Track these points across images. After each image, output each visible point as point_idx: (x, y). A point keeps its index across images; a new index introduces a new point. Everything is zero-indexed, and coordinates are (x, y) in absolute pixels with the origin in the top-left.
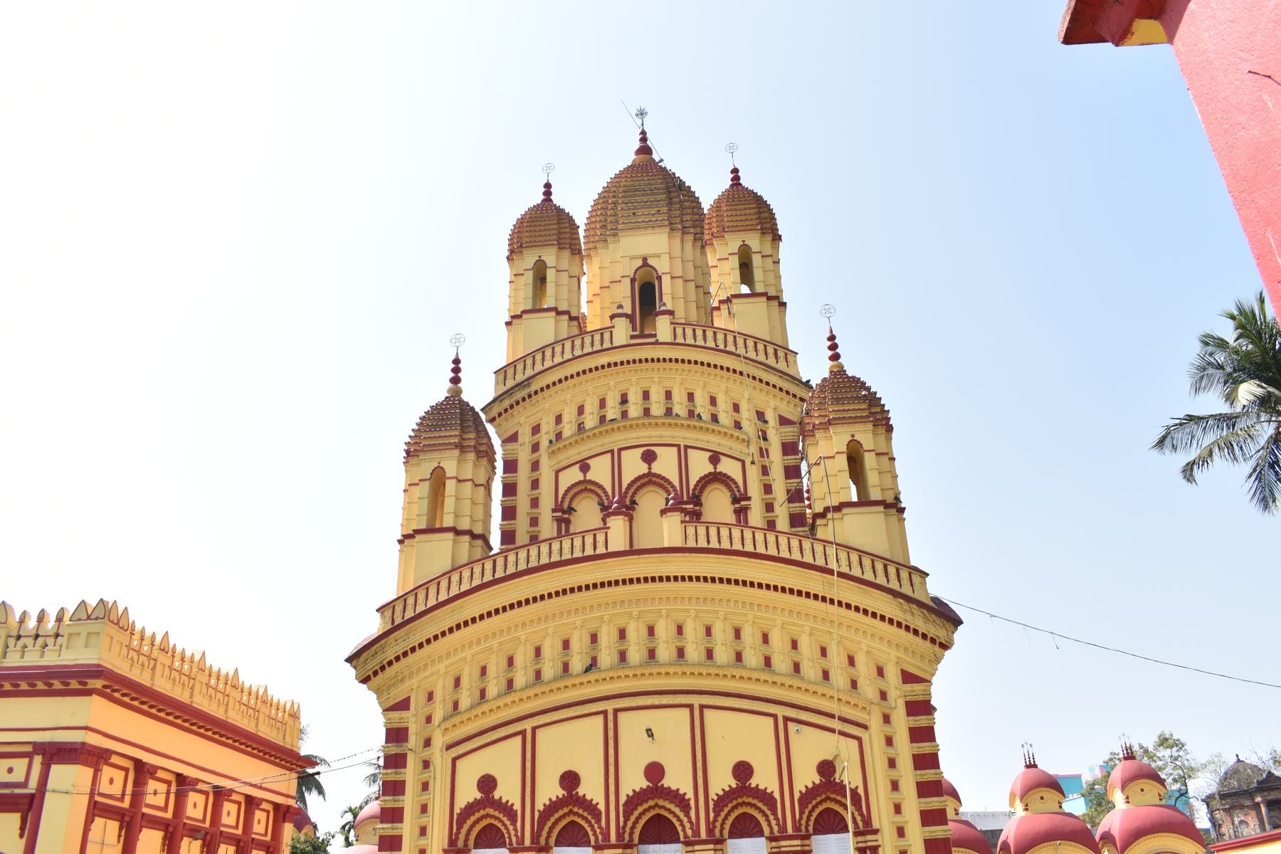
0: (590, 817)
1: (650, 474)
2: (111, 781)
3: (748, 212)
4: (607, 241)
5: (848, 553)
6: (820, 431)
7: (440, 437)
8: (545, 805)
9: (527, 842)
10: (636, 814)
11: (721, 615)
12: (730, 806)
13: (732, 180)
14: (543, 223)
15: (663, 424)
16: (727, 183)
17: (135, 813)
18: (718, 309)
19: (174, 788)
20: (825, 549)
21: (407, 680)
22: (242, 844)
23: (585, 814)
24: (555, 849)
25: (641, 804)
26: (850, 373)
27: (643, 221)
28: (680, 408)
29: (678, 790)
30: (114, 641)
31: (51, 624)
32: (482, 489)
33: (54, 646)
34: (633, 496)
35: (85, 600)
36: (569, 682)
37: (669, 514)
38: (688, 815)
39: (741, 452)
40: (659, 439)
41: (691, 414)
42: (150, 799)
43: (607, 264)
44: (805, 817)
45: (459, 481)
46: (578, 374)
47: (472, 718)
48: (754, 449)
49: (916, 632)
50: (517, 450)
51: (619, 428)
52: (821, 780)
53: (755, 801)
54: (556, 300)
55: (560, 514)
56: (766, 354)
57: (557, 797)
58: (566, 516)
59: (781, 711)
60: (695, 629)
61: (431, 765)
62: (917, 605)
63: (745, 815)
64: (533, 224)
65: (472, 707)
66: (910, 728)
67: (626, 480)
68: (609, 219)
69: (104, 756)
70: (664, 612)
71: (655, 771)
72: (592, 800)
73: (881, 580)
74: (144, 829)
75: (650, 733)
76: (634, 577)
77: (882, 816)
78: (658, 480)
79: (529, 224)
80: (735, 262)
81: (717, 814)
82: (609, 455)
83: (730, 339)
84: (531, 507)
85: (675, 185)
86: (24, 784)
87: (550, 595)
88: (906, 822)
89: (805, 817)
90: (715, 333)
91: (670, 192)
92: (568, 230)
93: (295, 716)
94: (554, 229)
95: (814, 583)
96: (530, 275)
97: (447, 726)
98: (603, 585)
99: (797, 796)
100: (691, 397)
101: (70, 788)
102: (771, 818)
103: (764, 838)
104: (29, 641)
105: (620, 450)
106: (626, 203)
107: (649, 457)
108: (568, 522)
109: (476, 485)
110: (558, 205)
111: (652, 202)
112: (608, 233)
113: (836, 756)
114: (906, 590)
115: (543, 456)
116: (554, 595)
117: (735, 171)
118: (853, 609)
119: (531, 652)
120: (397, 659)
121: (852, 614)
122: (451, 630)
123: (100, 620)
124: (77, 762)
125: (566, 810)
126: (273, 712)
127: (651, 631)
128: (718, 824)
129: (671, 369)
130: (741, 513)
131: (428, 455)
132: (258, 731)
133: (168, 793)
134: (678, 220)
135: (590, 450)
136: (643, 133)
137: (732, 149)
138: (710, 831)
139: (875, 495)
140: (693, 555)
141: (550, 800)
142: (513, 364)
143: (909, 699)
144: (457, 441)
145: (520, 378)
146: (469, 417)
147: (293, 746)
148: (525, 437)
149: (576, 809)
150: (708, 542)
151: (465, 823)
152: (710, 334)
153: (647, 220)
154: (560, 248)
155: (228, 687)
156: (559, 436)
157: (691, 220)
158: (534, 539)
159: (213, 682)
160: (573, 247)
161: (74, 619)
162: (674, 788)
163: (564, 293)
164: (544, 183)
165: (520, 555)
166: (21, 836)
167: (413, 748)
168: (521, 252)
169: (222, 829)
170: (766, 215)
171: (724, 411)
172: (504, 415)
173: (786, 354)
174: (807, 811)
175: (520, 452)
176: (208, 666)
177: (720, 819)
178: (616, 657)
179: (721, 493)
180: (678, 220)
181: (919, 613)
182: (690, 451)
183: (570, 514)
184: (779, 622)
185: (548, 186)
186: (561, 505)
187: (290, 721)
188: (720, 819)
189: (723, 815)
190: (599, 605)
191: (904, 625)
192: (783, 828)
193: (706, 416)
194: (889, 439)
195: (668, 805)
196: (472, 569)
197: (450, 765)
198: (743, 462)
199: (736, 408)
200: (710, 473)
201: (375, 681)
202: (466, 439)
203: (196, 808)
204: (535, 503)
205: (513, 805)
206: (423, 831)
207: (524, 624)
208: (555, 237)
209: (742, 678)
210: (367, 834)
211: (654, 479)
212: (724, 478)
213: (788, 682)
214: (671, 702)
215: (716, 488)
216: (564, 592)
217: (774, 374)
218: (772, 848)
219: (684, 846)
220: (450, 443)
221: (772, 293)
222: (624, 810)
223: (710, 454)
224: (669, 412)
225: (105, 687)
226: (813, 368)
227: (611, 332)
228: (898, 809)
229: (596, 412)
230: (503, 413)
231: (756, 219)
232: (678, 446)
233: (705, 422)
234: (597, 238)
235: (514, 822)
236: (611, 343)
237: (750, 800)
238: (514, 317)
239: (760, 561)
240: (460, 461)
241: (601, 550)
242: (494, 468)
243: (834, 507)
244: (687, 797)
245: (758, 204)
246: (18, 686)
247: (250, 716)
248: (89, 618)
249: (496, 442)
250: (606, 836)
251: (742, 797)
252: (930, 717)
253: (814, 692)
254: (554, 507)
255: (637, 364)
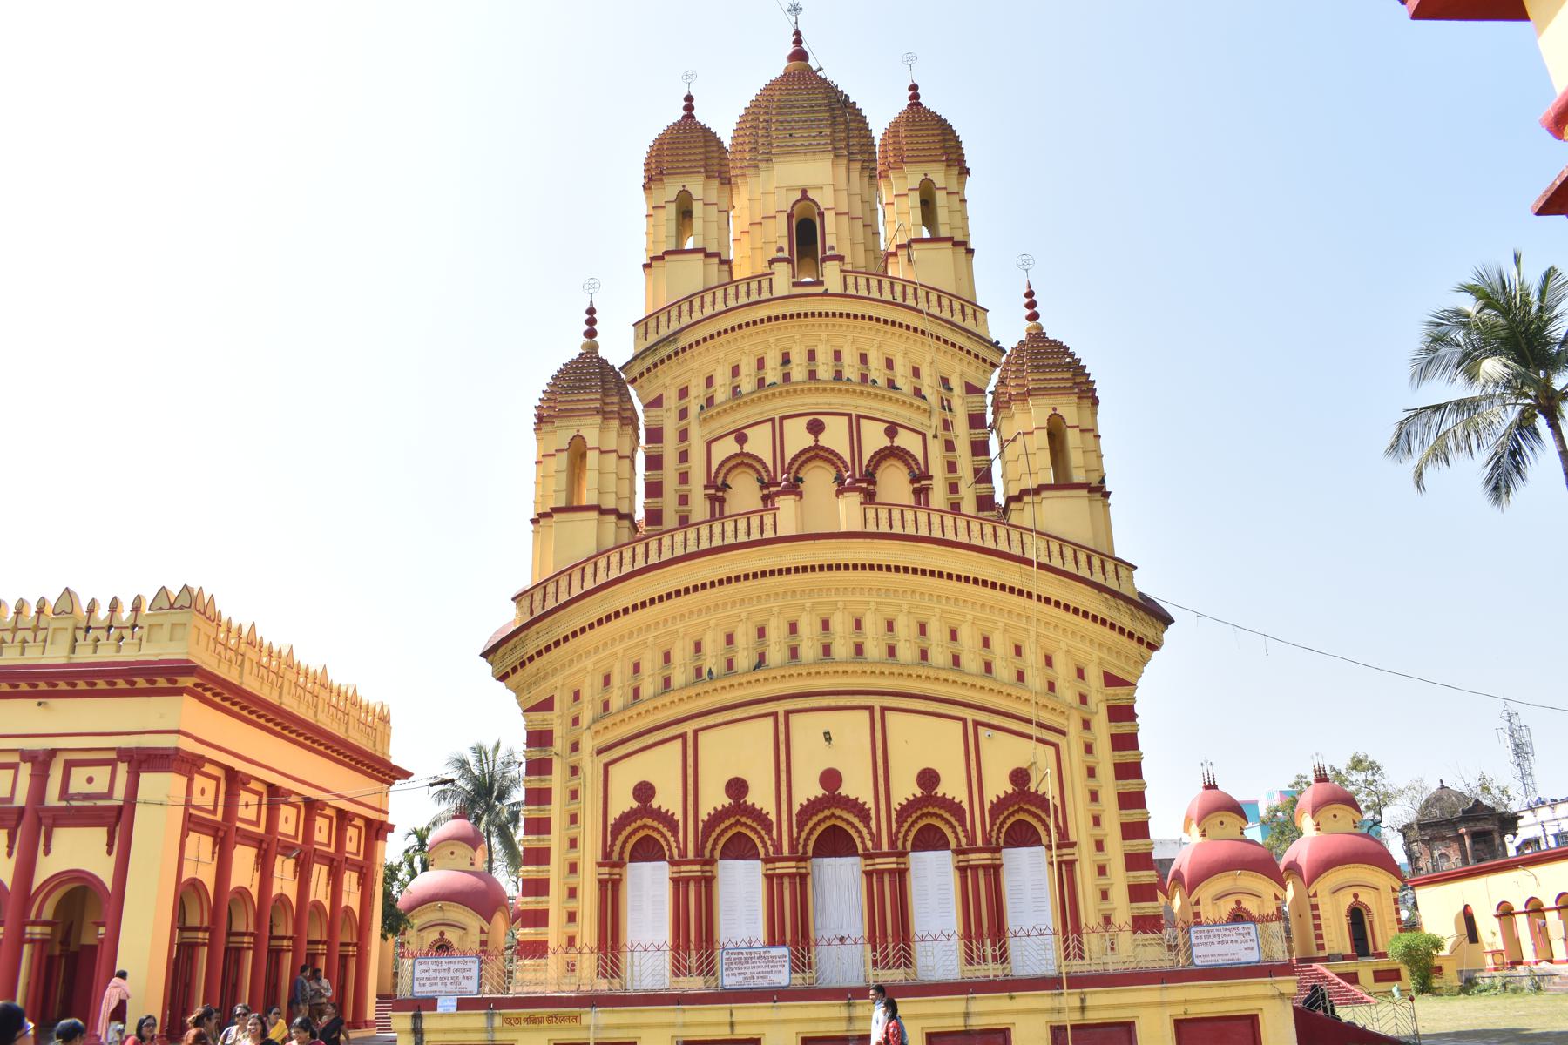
0: (759, 828)
1: (816, 447)
2: (203, 792)
3: (931, 139)
4: (757, 167)
5: (1048, 541)
6: (1017, 402)
7: (578, 400)
8: (709, 814)
9: (691, 855)
10: (810, 824)
11: (905, 608)
12: (914, 816)
13: (910, 98)
14: (687, 146)
15: (832, 390)
16: (904, 103)
17: (229, 828)
18: (895, 254)
19: (265, 799)
20: (1021, 537)
21: (551, 677)
22: (335, 863)
23: (754, 825)
24: (720, 862)
25: (816, 814)
26: (1051, 335)
27: (802, 145)
28: (851, 371)
29: (857, 799)
30: (202, 633)
31: (125, 614)
32: (628, 461)
33: (132, 639)
34: (797, 472)
35: (189, 585)
36: (735, 681)
37: (846, 494)
38: (868, 826)
39: (922, 424)
40: (827, 406)
41: (864, 378)
42: (242, 812)
43: (757, 196)
44: (996, 828)
45: (602, 452)
46: (733, 329)
47: (626, 719)
48: (936, 421)
49: (1121, 631)
50: (662, 416)
51: (781, 393)
52: (1014, 789)
53: (942, 812)
54: (704, 239)
55: (713, 491)
56: (952, 310)
57: (723, 806)
58: (720, 494)
59: (970, 715)
60: (876, 624)
61: (580, 770)
62: (1124, 602)
63: (929, 826)
64: (674, 146)
65: (625, 708)
66: (1111, 735)
67: (790, 453)
68: (761, 141)
69: (198, 763)
70: (840, 604)
71: (831, 778)
72: (762, 809)
73: (1084, 572)
74: (238, 846)
75: (828, 737)
76: (809, 564)
77: (1080, 829)
78: (826, 455)
79: (670, 146)
80: (914, 199)
81: (900, 825)
82: (769, 424)
83: (910, 291)
84: (680, 483)
85: (839, 101)
86: (109, 795)
87: (712, 584)
88: (1106, 835)
89: (996, 828)
90: (892, 284)
91: (833, 110)
92: (716, 155)
93: (385, 720)
94: (700, 153)
95: (1010, 574)
96: (672, 208)
97: (598, 728)
98: (772, 573)
99: (987, 806)
100: (863, 358)
101: (163, 798)
102: (959, 829)
103: (950, 852)
104: (102, 634)
105: (782, 419)
106: (782, 122)
107: (816, 428)
108: (722, 501)
109: (621, 457)
110: (702, 124)
111: (812, 121)
112: (759, 158)
113: (1032, 764)
114: (1112, 583)
115: (692, 423)
116: (717, 584)
117: (914, 87)
118: (1053, 603)
119: (691, 648)
120: (539, 653)
121: (1051, 609)
122: (600, 622)
123: (186, 610)
124: (171, 769)
125: (733, 820)
126: (363, 715)
127: (826, 625)
128: (901, 836)
129: (841, 325)
130: (921, 494)
131: (565, 422)
132: (348, 736)
133: (260, 804)
134: (843, 144)
135: (747, 417)
136: (797, 33)
137: (910, 60)
138: (892, 843)
139: (1078, 476)
140: (875, 541)
141: (715, 809)
142: (655, 315)
143: (1111, 703)
144: (598, 405)
145: (664, 332)
146: (610, 378)
147: (384, 754)
148: (671, 402)
149: (743, 820)
150: (891, 526)
151: (620, 834)
152: (886, 285)
153: (806, 143)
154: (708, 177)
155: (317, 687)
156: (710, 401)
157: (859, 144)
158: (684, 522)
159: (301, 680)
160: (723, 175)
161: (154, 607)
162: (852, 796)
163: (713, 231)
164: (684, 96)
165: (676, 539)
166: (109, 852)
167: (559, 752)
168: (661, 180)
169: (316, 846)
170: (953, 143)
171: (902, 376)
172: (646, 375)
173: (975, 311)
174: (998, 822)
175: (665, 419)
176: (296, 662)
177: (903, 830)
178: (787, 654)
179: (899, 471)
180: (843, 144)
181: (1126, 610)
182: (862, 421)
183: (724, 491)
184: (969, 617)
185: (689, 98)
186: (715, 482)
187: (380, 726)
188: (903, 830)
189: (906, 825)
190: (768, 596)
191: (1108, 622)
192: (971, 841)
193: (882, 382)
194: (1094, 413)
195: (846, 815)
196: (621, 553)
197: (601, 771)
198: (924, 436)
199: (916, 372)
200: (886, 447)
201: (514, 678)
202: (608, 404)
203: (288, 822)
204: (684, 478)
205: (673, 814)
206: (573, 843)
207: (682, 616)
208: (702, 163)
209: (928, 677)
210: (443, 858)
211: (821, 453)
212: (902, 454)
213: (979, 682)
214: (849, 704)
215: (892, 465)
216: (729, 580)
217: (962, 334)
218: (959, 862)
219: (862, 859)
220: (590, 408)
221: (959, 238)
222: (797, 820)
223: (887, 425)
224: (838, 375)
225: (197, 685)
226: (1008, 329)
227: (771, 279)
228: (1097, 821)
229: (753, 374)
230: (645, 373)
231: (941, 148)
232: (849, 415)
233: (880, 388)
234: (746, 164)
235: (675, 833)
236: (771, 292)
237: (936, 810)
238: (654, 259)
239: (950, 549)
240: (602, 429)
241: (769, 534)
242: (638, 437)
243: (1033, 490)
244: (866, 807)
245: (944, 129)
246: (115, 684)
247: (339, 720)
248: (172, 606)
249: (639, 406)
250: (778, 848)
251: (927, 807)
252: (1133, 723)
253: (1008, 695)
254: (706, 483)
255: (802, 319)
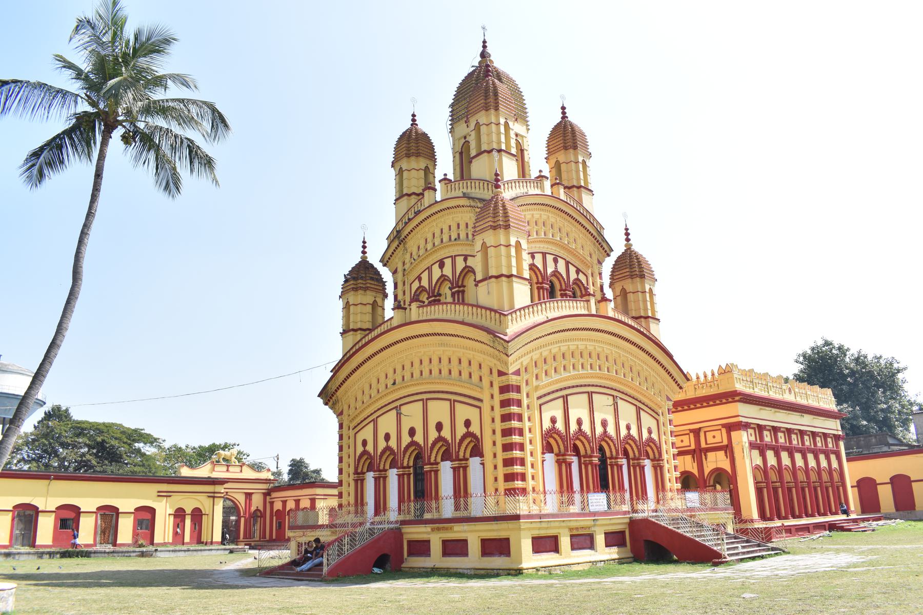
107: (556, 261)
